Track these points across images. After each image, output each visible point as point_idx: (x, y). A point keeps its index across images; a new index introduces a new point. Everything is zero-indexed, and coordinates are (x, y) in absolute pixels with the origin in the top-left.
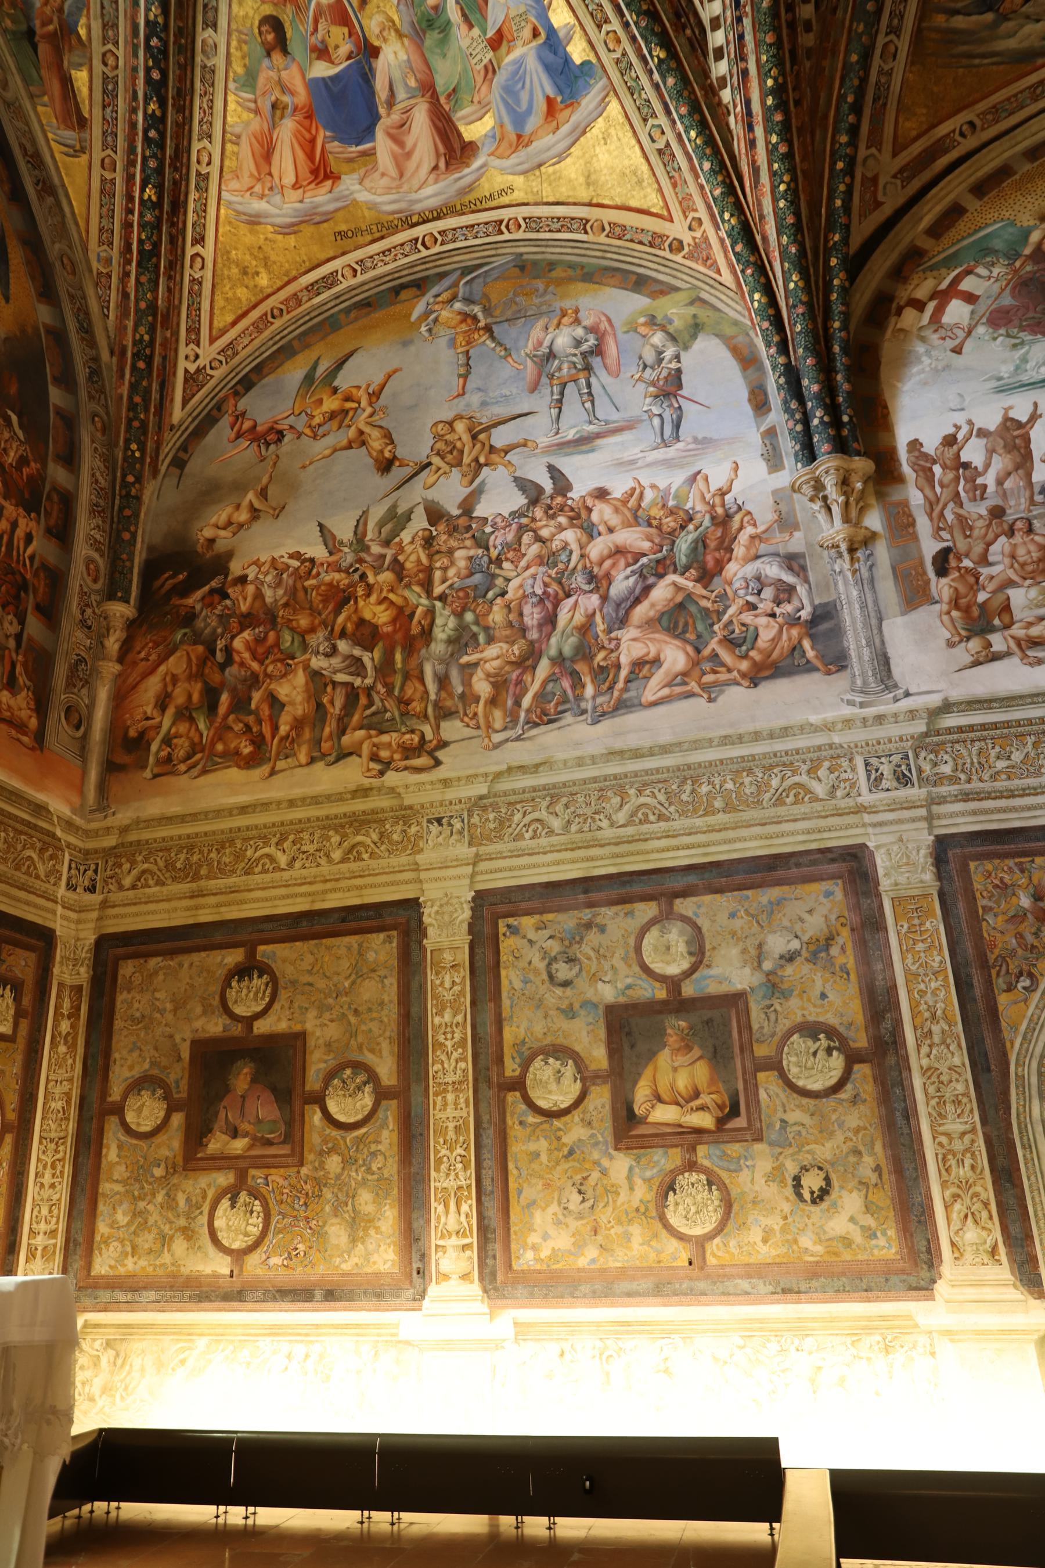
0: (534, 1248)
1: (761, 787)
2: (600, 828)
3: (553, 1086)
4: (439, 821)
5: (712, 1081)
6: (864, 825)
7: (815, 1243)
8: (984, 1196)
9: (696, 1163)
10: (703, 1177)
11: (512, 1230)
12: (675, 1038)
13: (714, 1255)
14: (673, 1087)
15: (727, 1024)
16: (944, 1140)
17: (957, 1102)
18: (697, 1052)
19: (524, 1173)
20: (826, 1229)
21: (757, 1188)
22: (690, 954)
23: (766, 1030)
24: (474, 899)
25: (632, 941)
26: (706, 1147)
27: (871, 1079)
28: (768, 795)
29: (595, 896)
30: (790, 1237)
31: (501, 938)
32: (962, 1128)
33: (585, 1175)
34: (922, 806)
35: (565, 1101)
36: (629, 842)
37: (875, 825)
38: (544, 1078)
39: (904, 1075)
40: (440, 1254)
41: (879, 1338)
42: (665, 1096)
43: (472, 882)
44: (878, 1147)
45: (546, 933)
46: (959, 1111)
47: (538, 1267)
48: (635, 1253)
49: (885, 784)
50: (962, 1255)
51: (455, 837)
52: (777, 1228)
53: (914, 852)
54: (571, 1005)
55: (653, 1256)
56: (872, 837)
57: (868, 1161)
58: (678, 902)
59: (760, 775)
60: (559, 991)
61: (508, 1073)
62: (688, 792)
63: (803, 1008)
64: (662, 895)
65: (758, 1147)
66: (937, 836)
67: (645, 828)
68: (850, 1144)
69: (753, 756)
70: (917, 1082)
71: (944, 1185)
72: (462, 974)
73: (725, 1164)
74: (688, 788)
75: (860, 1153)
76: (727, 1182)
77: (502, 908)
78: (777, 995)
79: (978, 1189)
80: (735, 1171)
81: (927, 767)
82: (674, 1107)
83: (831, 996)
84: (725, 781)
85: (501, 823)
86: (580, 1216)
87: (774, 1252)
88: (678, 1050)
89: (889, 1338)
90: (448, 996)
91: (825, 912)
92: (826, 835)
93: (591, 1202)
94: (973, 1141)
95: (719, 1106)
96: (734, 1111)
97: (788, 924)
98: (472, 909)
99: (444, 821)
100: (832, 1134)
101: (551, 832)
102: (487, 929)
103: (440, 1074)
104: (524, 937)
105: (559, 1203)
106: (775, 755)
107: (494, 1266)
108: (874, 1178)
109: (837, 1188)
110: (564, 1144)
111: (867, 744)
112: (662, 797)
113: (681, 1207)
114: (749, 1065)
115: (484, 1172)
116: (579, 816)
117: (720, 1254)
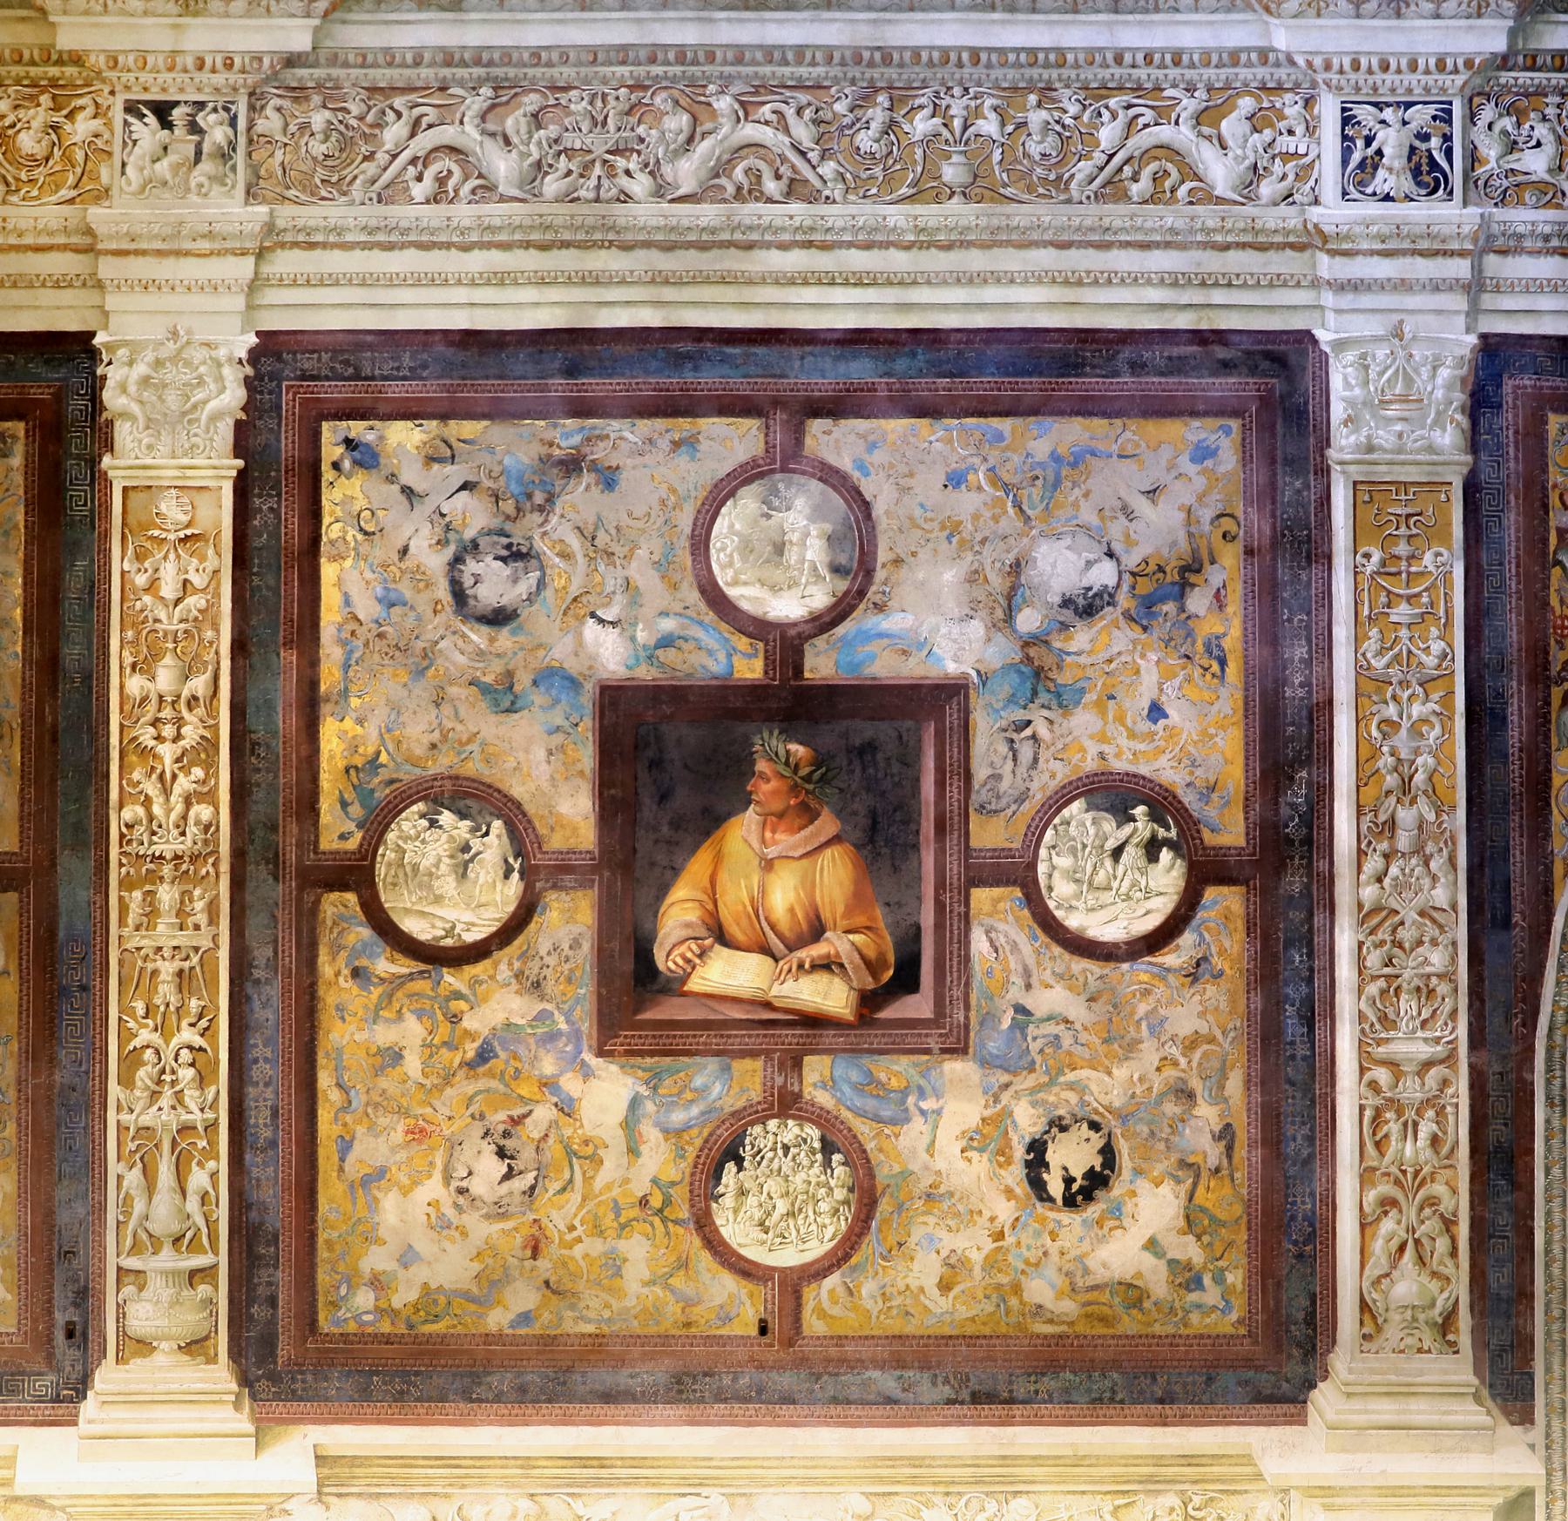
0: (377, 1283)
1: (1074, 140)
2: (625, 197)
3: (447, 884)
4: (162, 111)
5: (857, 901)
6: (1316, 284)
7: (1060, 1295)
8: (1446, 1205)
9: (798, 1096)
10: (813, 1133)
12: (774, 784)
13: (822, 1314)
14: (757, 907)
15: (909, 760)
16: (1382, 1075)
17: (1425, 992)
18: (827, 825)
19: (359, 1100)
20: (1091, 1263)
21: (940, 1164)
22: (836, 570)
23: (1004, 785)
24: (255, 356)
26: (826, 1060)
27: (1240, 925)
28: (1084, 168)
29: (597, 386)
30: (1004, 1279)
31: (328, 474)
32: (1424, 1051)
33: (517, 1112)
34: (1462, 254)
35: (477, 927)
36: (703, 247)
37: (1341, 287)
38: (426, 863)
39: (1318, 920)
40: (129, 1290)
41: (1172, 1500)
42: (735, 931)
43: (250, 307)
44: (1235, 1084)
45: (456, 473)
46: (1425, 1014)
47: (386, 1327)
48: (630, 1302)
49: (1383, 181)
50: (1379, 1329)
51: (206, 166)
52: (976, 1257)
53: (1425, 372)
54: (510, 674)
55: (673, 1309)
56: (1330, 317)
57: (1207, 1114)
58: (816, 426)
59: (1073, 109)
60: (478, 636)
61: (328, 842)
62: (875, 126)
63: (1102, 738)
64: (777, 403)
65: (955, 1067)
66: (1484, 337)
67: (751, 211)
68: (1170, 1073)
69: (1061, 52)
70: (1345, 939)
71: (1367, 1176)
72: (211, 563)
73: (871, 1104)
74: (877, 115)
75: (1191, 1096)
76: (870, 1146)
77: (336, 391)
78: (1044, 697)
79: (1439, 1189)
80: (893, 1122)
81: (1490, 151)
82: (755, 961)
83: (1174, 715)
84: (978, 113)
85: (346, 144)
86: (499, 1211)
87: (964, 1312)
88: (781, 815)
89: (1197, 1500)
90: (169, 622)
91: (1188, 499)
92: (1218, 297)
93: (530, 1178)
94: (1445, 1083)
95: (868, 963)
96: (906, 979)
97: (1092, 519)
98: (248, 382)
99: (177, 114)
100: (1132, 1047)
101: (487, 190)
102: (288, 445)
103: (140, 830)
104: (392, 478)
105: (447, 1178)
106: (1119, 60)
107: (272, 1322)
108: (1213, 1154)
109: (1126, 1174)
110: (468, 1034)
111: (1356, 66)
112: (803, 132)
113: (751, 1201)
114: (954, 867)
115: (251, 1091)
116: (569, 152)
117: (835, 1311)
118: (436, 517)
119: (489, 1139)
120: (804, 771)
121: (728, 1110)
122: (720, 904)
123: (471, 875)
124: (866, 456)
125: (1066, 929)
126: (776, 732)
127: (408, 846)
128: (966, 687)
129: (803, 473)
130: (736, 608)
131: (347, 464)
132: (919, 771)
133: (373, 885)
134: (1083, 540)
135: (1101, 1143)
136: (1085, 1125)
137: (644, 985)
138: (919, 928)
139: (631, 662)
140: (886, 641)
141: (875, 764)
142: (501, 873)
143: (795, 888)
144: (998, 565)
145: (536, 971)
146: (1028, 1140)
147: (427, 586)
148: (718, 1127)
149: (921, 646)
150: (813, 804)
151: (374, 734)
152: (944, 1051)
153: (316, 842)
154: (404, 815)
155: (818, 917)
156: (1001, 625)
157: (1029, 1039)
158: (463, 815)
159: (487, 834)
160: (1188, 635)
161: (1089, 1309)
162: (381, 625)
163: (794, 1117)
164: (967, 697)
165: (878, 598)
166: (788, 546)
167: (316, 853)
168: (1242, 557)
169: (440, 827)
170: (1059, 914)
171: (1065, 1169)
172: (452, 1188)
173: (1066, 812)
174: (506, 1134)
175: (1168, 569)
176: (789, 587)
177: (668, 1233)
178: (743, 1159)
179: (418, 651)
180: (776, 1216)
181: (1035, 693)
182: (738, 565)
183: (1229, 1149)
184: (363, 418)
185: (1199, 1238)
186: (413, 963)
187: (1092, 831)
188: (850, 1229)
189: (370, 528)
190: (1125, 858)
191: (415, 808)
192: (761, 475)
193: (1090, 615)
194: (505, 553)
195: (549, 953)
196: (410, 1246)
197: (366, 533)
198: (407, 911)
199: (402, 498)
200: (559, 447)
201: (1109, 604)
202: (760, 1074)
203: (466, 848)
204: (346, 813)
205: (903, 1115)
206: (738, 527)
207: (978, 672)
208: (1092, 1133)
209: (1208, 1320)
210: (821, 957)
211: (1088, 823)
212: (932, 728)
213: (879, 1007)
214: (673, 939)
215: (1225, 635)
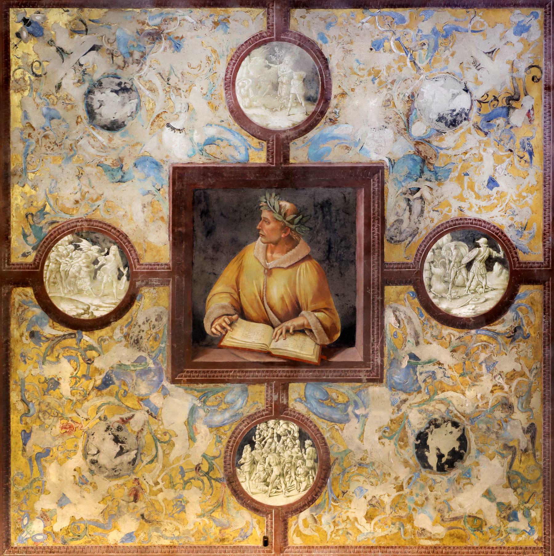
0: (45, 516)
3: (85, 283)
5: (320, 294)
7: (435, 523)
9: (286, 407)
10: (294, 428)
11: (13, 490)
12: (272, 225)
13: (299, 533)
14: (263, 296)
19: (34, 408)
20: (453, 505)
21: (366, 446)
22: (308, 99)
23: (404, 226)
25: (221, 69)
26: (302, 385)
27: (540, 308)
30: (403, 513)
31: (14, 40)
33: (126, 415)
38: (73, 271)
42: (250, 311)
44: (536, 401)
45: (88, 40)
47: (50, 543)
48: (190, 527)
52: (387, 500)
54: (121, 160)
55: (214, 531)
60: (103, 137)
61: (16, 258)
63: (461, 198)
65: (375, 390)
73: (327, 411)
76: (326, 435)
78: (427, 174)
80: (340, 422)
82: (262, 327)
83: (504, 183)
86: (115, 474)
87: (380, 533)
91: (512, 57)
93: (133, 454)
97: (457, 70)
100: (477, 378)
104: (51, 43)
105: (85, 455)
108: (524, 441)
109: (473, 452)
110: (97, 370)
113: (259, 467)
114: (375, 273)
117: (307, 532)
118: (77, 66)
119: (109, 432)
120: (289, 218)
121: (246, 414)
122: (241, 294)
123: (99, 277)
124: (325, 31)
125: (439, 310)
126: (274, 195)
127: (63, 261)
128: (382, 168)
129: (290, 41)
130: (250, 122)
131: (25, 34)
132: (356, 217)
133: (42, 283)
134: (450, 81)
135: (459, 434)
136: (450, 424)
137: (198, 342)
138: (355, 309)
139: (191, 153)
140: (337, 141)
141: (330, 214)
142: (116, 277)
143: (285, 286)
144: (401, 96)
145: (136, 333)
146: (417, 432)
147: (72, 107)
148: (240, 424)
149: (356, 144)
150: (295, 237)
151: (43, 195)
152: (369, 380)
153: (9, 258)
154: (60, 242)
155: (298, 303)
156: (403, 132)
157: (418, 373)
158: (94, 243)
159: (108, 253)
160: (511, 138)
161: (452, 531)
162: (46, 130)
163: (284, 419)
164: (383, 174)
165: (332, 116)
166: (280, 84)
167: (9, 264)
168: (543, 91)
169: (81, 249)
170: (435, 301)
171: (438, 449)
172: (88, 460)
173: (439, 242)
174: (119, 429)
175: (500, 99)
176: (281, 109)
177: (212, 486)
178: (254, 443)
179: (67, 146)
180: (273, 476)
181: (422, 172)
182: (252, 95)
183: (533, 438)
184: (34, 6)
185: (515, 490)
186: (65, 329)
187: (454, 253)
188: (315, 484)
189: (38, 72)
190: (473, 268)
191: (66, 238)
192: (265, 42)
193: (454, 126)
194: (118, 88)
195: (144, 323)
196: (64, 495)
197: (36, 75)
198: (62, 298)
199: (57, 55)
200: (148, 25)
201: (465, 119)
202: (264, 393)
203: (96, 262)
204: (26, 241)
205: (346, 418)
206: (251, 73)
207: (390, 160)
208: (453, 428)
209: (520, 539)
210: (299, 326)
211: (452, 249)
212: (362, 194)
213: (332, 355)
214: (215, 315)
215: (532, 137)
